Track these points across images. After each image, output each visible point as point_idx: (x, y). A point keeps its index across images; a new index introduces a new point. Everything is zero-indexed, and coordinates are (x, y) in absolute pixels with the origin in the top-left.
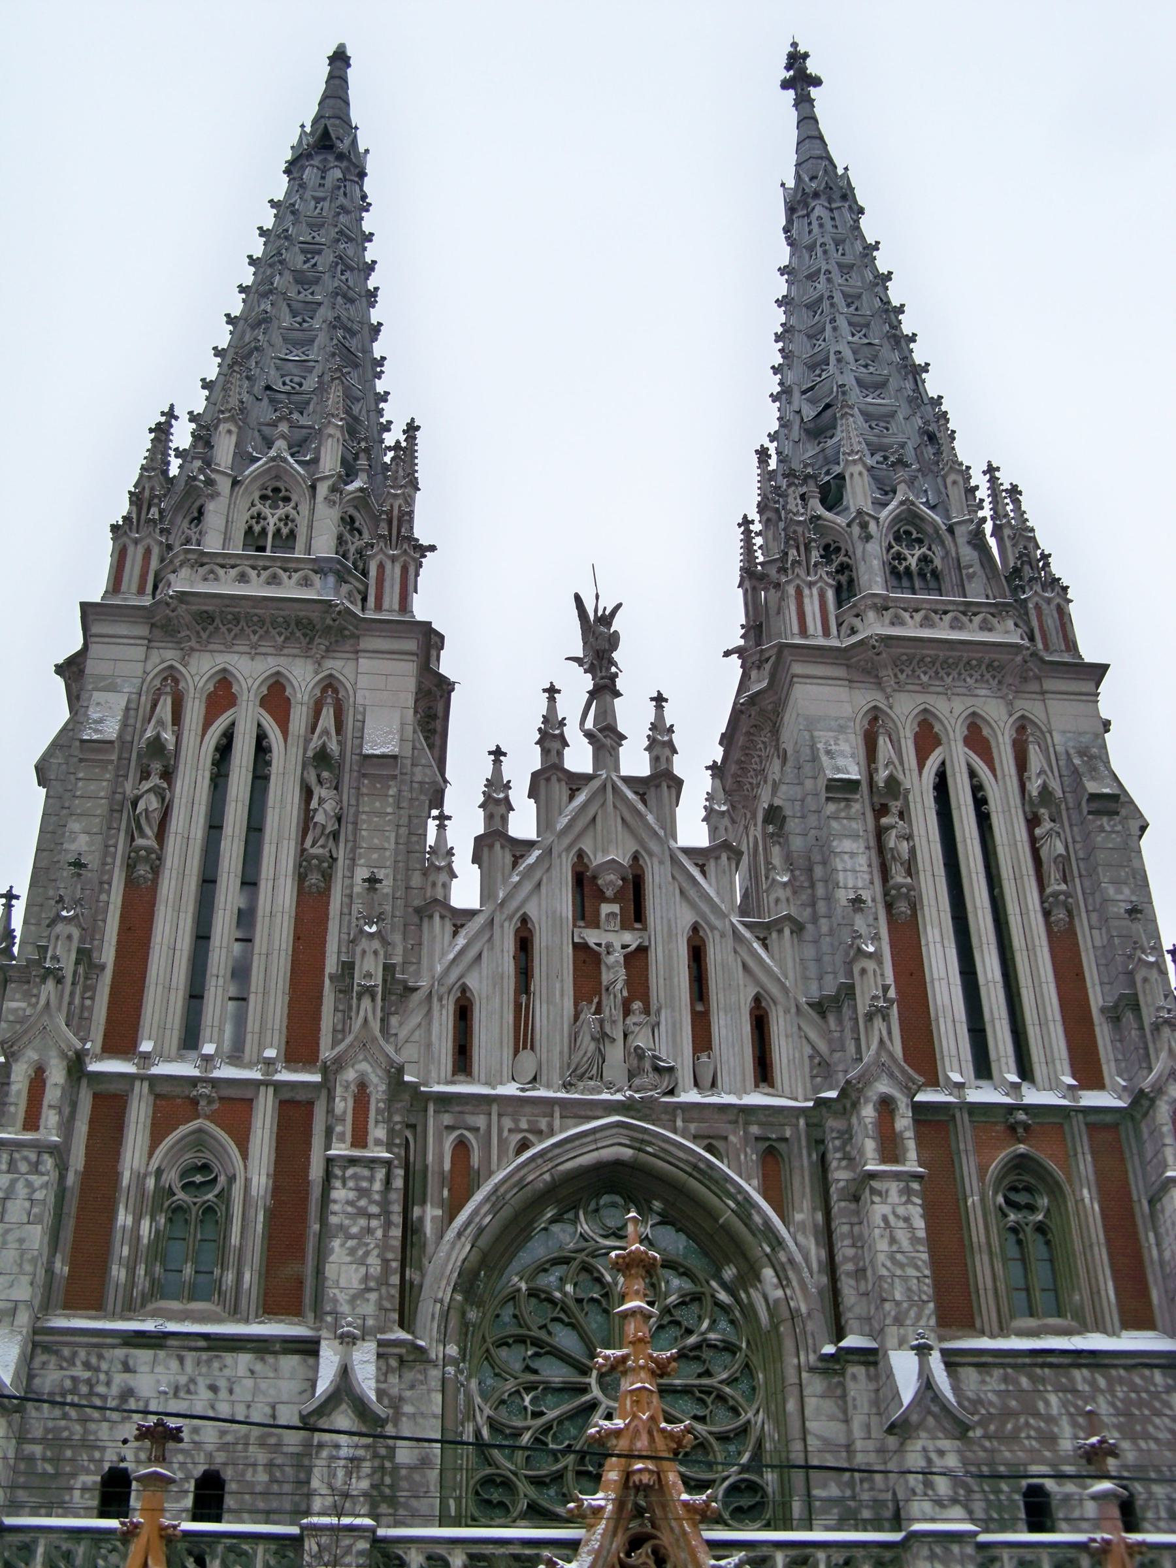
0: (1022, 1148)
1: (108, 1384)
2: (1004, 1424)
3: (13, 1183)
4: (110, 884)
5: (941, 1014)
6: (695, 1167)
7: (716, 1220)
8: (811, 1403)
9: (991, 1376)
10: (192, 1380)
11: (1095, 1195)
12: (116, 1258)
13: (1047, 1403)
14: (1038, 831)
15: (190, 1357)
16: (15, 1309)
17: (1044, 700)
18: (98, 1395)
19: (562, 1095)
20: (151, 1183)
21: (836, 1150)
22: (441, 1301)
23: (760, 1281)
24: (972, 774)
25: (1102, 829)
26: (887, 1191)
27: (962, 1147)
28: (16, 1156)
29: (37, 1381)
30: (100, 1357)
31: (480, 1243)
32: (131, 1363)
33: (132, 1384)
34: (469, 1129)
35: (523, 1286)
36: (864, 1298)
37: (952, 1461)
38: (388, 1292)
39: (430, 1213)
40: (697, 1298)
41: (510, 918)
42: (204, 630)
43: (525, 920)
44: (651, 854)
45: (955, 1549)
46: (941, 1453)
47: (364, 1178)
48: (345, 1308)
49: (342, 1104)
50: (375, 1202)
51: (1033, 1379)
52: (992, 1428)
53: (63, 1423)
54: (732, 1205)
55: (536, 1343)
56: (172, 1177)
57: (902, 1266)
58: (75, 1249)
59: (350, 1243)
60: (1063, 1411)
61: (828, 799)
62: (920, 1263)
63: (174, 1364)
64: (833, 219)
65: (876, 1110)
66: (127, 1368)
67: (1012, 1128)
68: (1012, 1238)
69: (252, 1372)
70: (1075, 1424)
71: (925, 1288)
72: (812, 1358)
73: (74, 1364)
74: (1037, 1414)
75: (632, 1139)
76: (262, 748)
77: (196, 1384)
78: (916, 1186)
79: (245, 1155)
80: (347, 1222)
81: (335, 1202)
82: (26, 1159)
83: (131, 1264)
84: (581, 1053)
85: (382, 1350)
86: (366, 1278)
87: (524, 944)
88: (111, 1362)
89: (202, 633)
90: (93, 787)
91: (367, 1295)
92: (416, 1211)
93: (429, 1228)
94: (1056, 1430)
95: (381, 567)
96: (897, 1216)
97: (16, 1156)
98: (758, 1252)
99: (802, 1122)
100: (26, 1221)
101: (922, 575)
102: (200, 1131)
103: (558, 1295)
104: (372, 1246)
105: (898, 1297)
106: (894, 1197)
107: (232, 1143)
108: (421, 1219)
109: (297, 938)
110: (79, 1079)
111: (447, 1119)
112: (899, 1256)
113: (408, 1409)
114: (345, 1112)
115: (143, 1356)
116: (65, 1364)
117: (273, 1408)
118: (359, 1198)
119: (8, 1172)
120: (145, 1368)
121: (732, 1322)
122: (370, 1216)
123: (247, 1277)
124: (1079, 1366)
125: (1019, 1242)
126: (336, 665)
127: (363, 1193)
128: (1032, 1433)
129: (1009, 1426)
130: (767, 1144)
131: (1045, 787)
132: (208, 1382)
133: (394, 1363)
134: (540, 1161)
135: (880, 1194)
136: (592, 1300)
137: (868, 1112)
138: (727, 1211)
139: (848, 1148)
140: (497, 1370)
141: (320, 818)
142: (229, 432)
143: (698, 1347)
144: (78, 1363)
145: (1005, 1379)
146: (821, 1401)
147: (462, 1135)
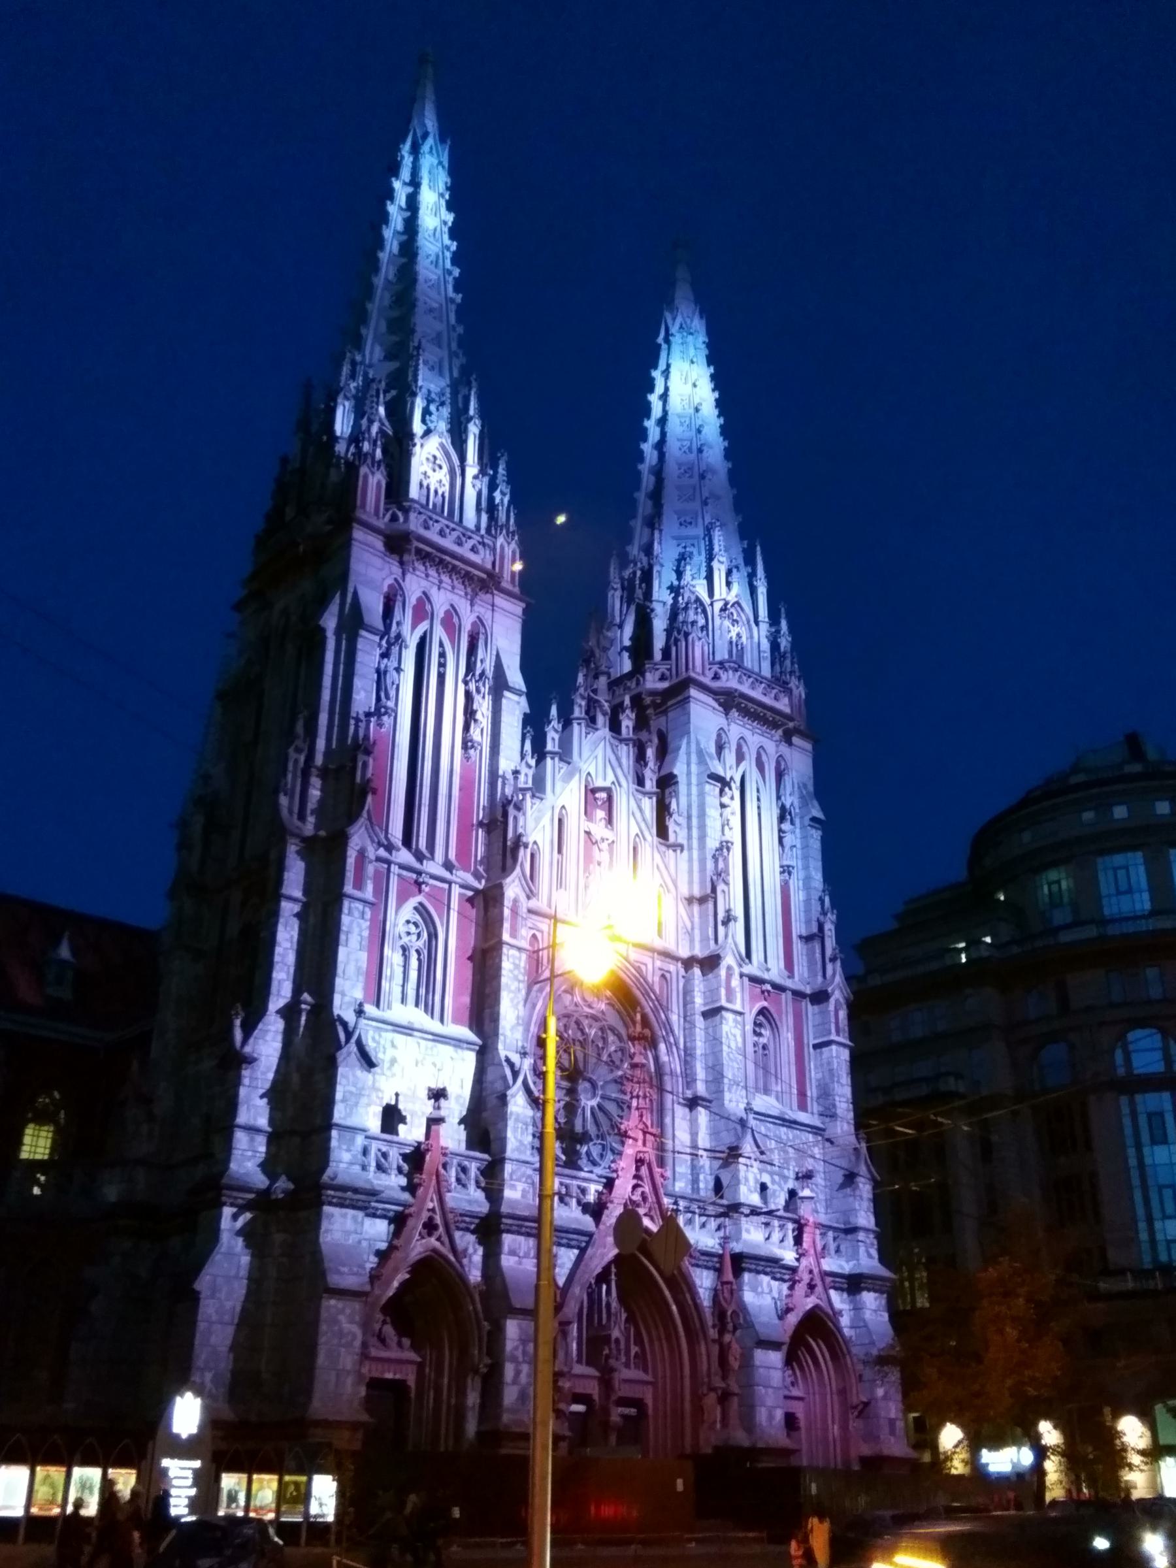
0: (765, 1004)
1: (384, 1053)
8: (677, 1121)
14: (783, 826)
15: (423, 1042)
34: (538, 930)
67: (763, 992)
70: (779, 1155)
97: (352, 905)
98: (659, 1033)
101: (737, 645)
103: (566, 1035)
106: (731, 1023)
112: (731, 1055)
115: (400, 1039)
122: (520, 981)
124: (783, 1126)
126: (482, 610)
136: (597, 1046)
143: (621, 1077)
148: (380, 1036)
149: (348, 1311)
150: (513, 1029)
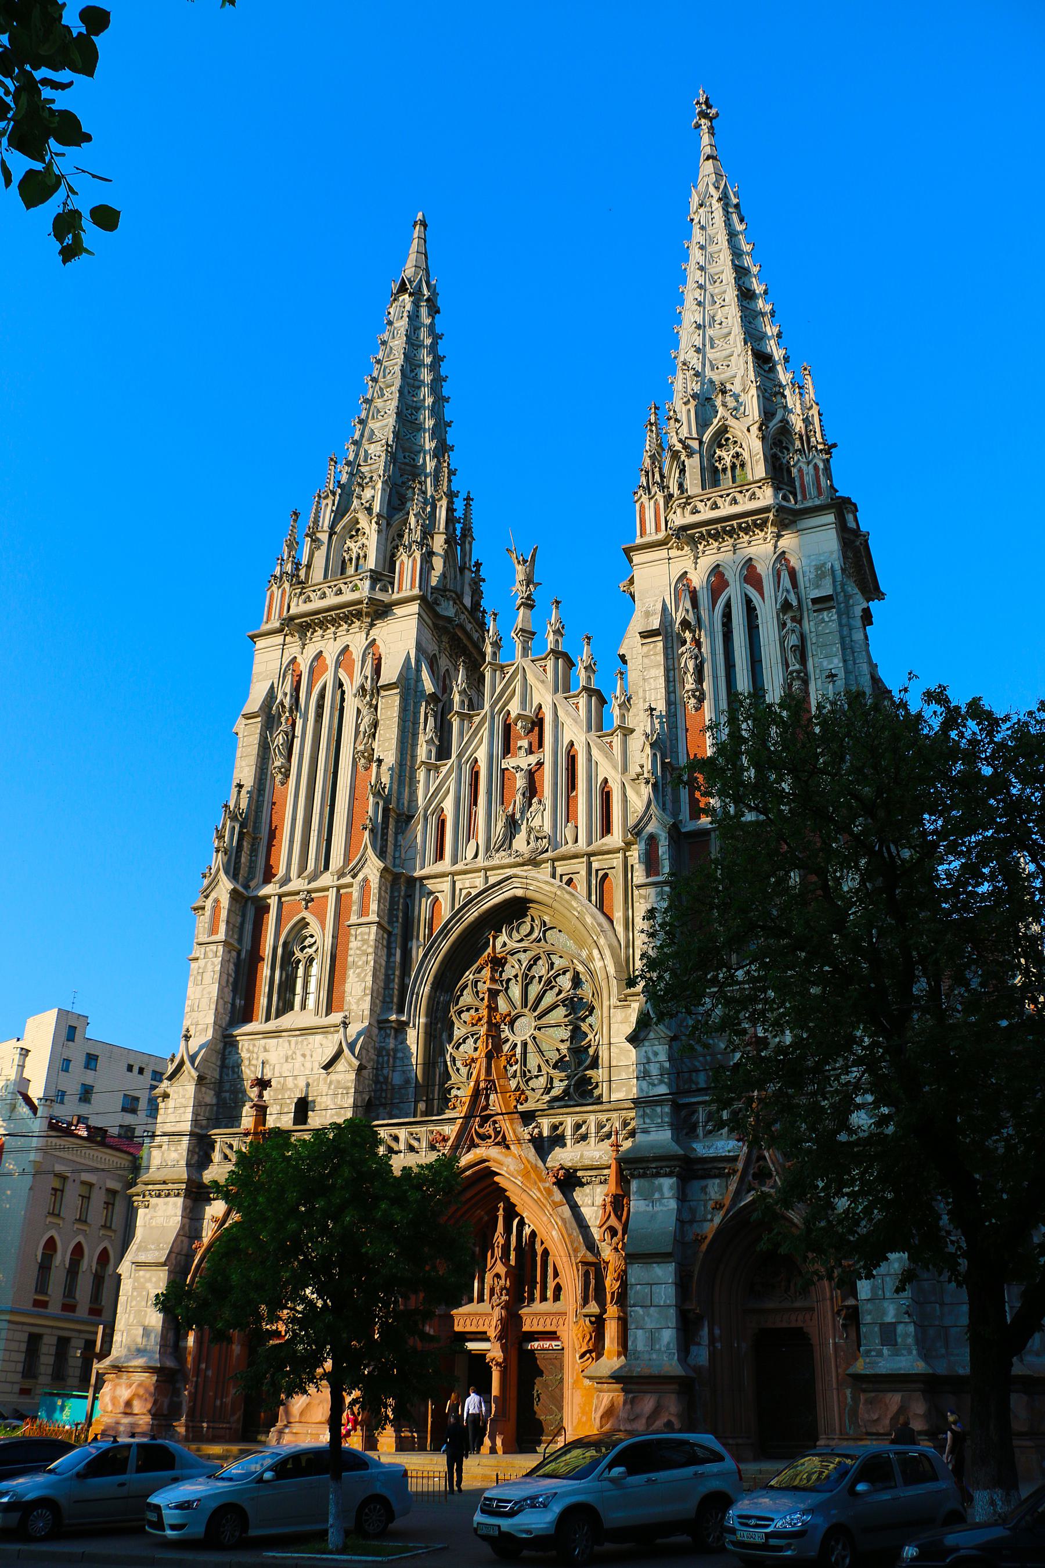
1: (257, 1059)
3: (206, 963)
10: (294, 1053)
19: (486, 864)
24: (749, 601)
25: (823, 621)
28: (207, 949)
29: (227, 1061)
33: (267, 1058)
37: (663, 1057)
43: (476, 761)
45: (659, 1109)
46: (656, 1054)
47: (365, 934)
48: (354, 1007)
50: (371, 946)
54: (576, 914)
59: (358, 971)
63: (286, 1045)
65: (646, 845)
66: (266, 1050)
79: (323, 929)
82: (211, 950)
85: (381, 1025)
90: (251, 739)
108: (411, 948)
118: (363, 946)
120: (274, 1049)
127: (365, 941)
131: (786, 600)
133: (388, 1031)
148: (254, 1045)
149: (154, 1280)
150: (357, 1003)
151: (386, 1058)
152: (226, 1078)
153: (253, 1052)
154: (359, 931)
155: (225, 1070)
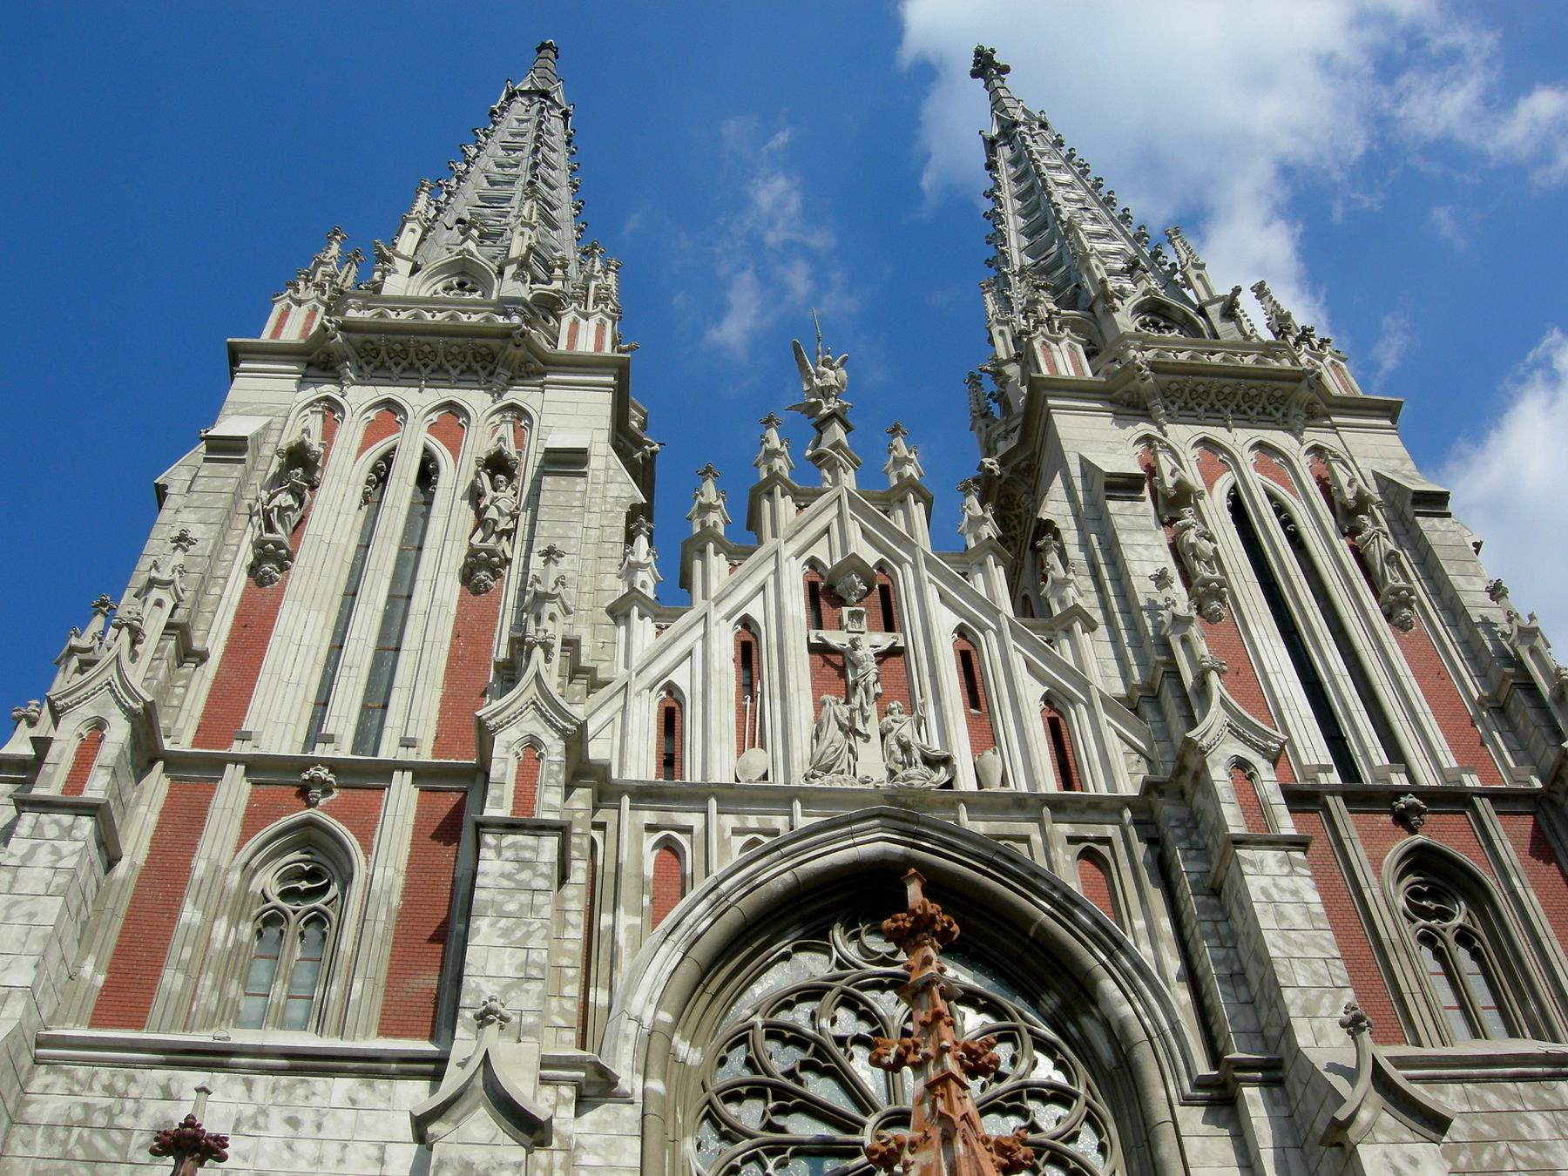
0: (1419, 838)
1: (136, 1114)
2: (1477, 1155)
4: (226, 579)
5: (1283, 705)
6: (990, 863)
7: (1026, 934)
9: (1447, 1095)
11: (1527, 884)
12: (171, 960)
13: (1530, 1125)
15: (262, 1082)
16: (8, 995)
17: (1337, 433)
18: (120, 1129)
20: (235, 878)
21: (1181, 839)
22: (639, 1021)
23: (1095, 1003)
24: (1271, 497)
26: (1262, 862)
27: (1343, 834)
28: (44, 818)
29: (32, 1109)
30: (131, 1079)
31: (693, 953)
32: (174, 1088)
35: (758, 1020)
36: (1248, 1008)
38: (561, 1006)
39: (624, 922)
40: (1007, 1036)
41: (728, 617)
42: (368, 363)
44: (900, 562)
47: (525, 848)
49: (502, 765)
50: (542, 875)
51: (1504, 1095)
52: (1462, 1160)
53: (62, 1164)
55: (780, 1092)
56: (268, 881)
57: (1300, 946)
58: (121, 952)
59: (504, 922)
60: (1557, 1135)
61: (1110, 498)
62: (1324, 943)
64: (1035, 141)
66: (167, 1094)
68: (1426, 952)
69: (353, 1101)
71: (1338, 972)
72: (1186, 1083)
73: (91, 1088)
74: (1522, 1141)
75: (902, 832)
76: (427, 475)
77: (268, 1115)
78: (1298, 855)
79: (367, 850)
80: (500, 898)
81: (485, 874)
82: (57, 822)
83: (194, 973)
84: (826, 743)
85: (547, 1072)
86: (527, 964)
87: (747, 654)
88: (146, 1086)
89: (365, 367)
90: (217, 483)
91: (526, 986)
92: (606, 919)
93: (622, 937)
94: (1552, 1159)
95: (575, 324)
96: (1281, 889)
98: (1091, 962)
99: (1128, 814)
100: (41, 890)
102: (309, 823)
103: (809, 1030)
104: (536, 926)
105: (1302, 983)
107: (352, 837)
109: (456, 635)
110: (152, 763)
111: (649, 817)
113: (587, 1159)
114: (504, 774)
116: (77, 1088)
117: (382, 1149)
118: (519, 871)
119: (30, 837)
121: (1059, 1065)
123: (357, 985)
125: (1439, 954)
127: (523, 863)
128: (1521, 1165)
129: (1486, 1157)
130: (1084, 845)
132: (286, 1114)
133: (568, 1092)
134: (777, 853)
135: (1253, 864)
137: (1219, 774)
138: (1040, 911)
139: (1194, 838)
140: (724, 1128)
141: (492, 513)
142: (413, 231)
143: (1015, 1094)
144: (97, 1086)
145: (1467, 1098)
146: (1208, 1141)
147: (668, 838)
151: (559, 1157)
152: (20, 1151)
153: (123, 1096)
154: (510, 839)
155: (21, 1131)
